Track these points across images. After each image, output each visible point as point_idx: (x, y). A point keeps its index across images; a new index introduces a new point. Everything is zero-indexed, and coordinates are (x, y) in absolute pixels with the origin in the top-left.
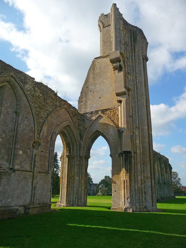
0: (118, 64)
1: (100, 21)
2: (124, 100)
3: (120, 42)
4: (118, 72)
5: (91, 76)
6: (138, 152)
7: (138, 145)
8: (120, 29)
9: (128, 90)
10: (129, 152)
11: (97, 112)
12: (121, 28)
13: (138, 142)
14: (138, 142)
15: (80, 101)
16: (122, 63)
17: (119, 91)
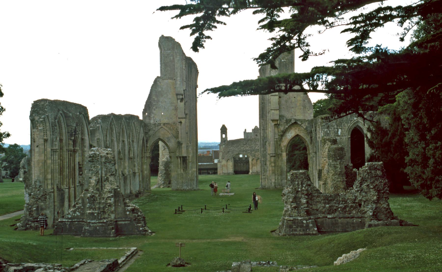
0: (181, 97)
1: (160, 38)
2: (183, 121)
3: (183, 79)
4: (180, 101)
5: (154, 93)
6: (190, 156)
7: (190, 151)
8: (183, 68)
9: (186, 115)
10: (186, 157)
11: (160, 124)
12: (184, 67)
13: (190, 149)
14: (190, 149)
15: (144, 113)
16: (183, 97)
17: (181, 116)
